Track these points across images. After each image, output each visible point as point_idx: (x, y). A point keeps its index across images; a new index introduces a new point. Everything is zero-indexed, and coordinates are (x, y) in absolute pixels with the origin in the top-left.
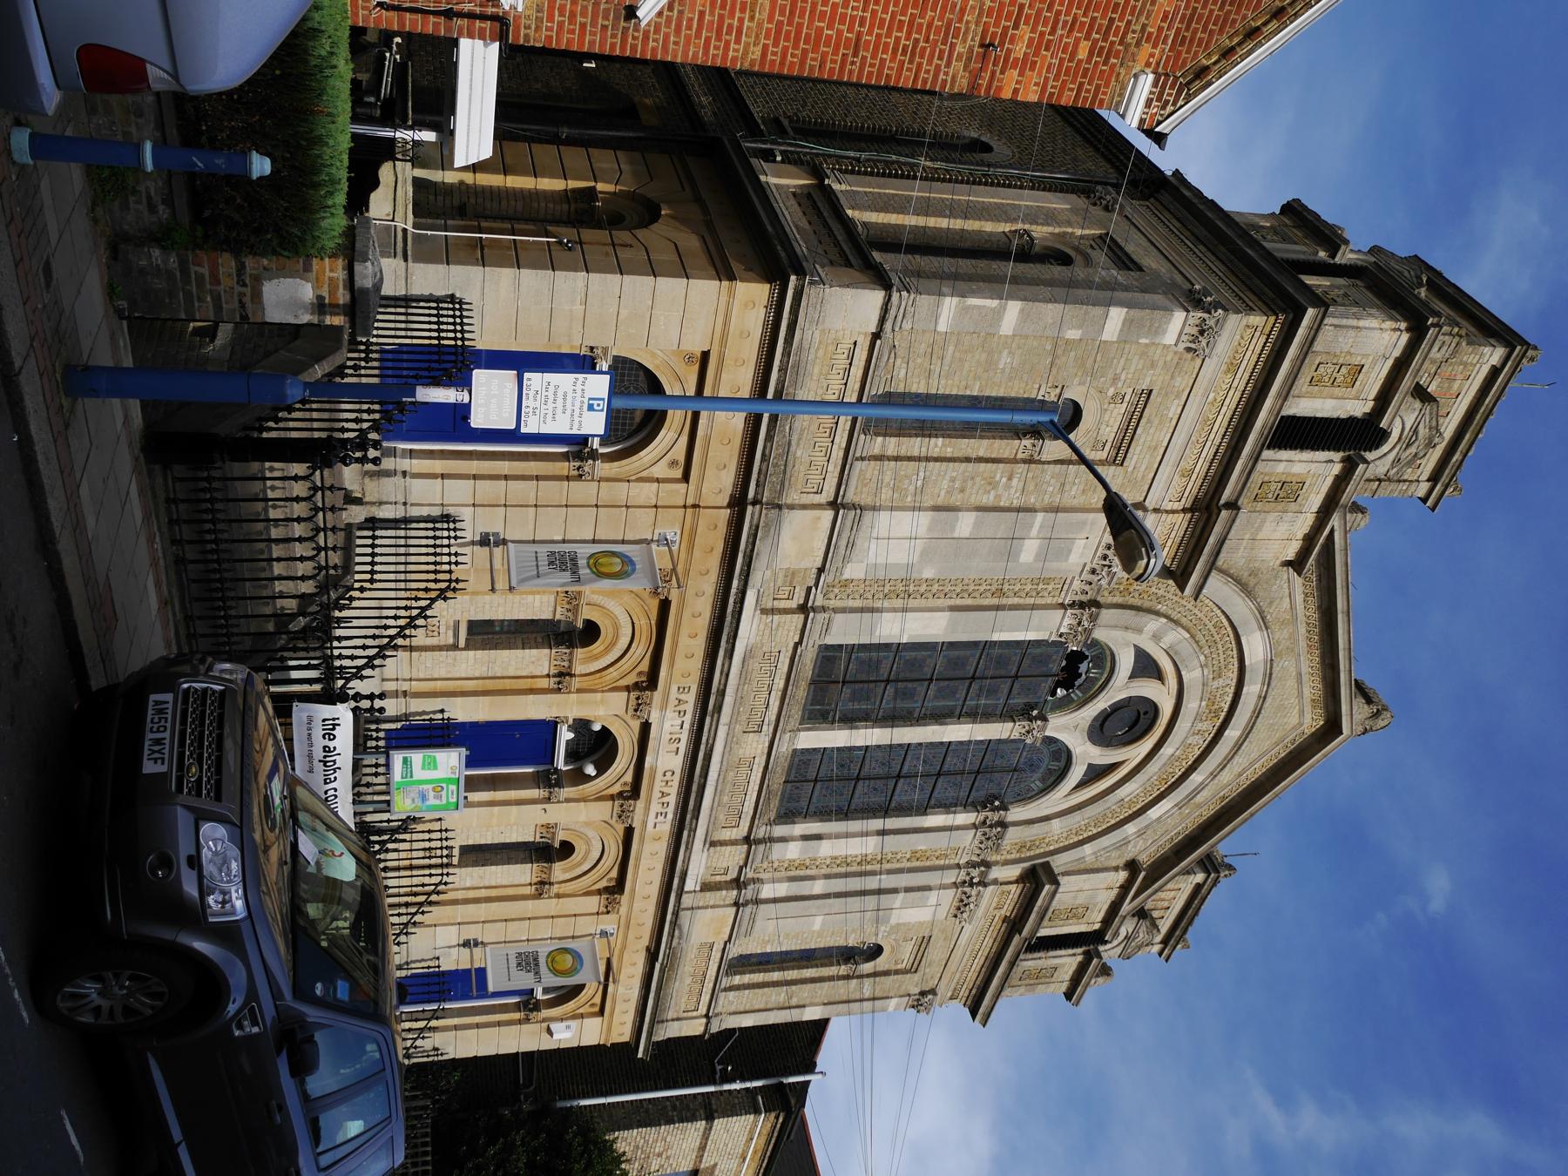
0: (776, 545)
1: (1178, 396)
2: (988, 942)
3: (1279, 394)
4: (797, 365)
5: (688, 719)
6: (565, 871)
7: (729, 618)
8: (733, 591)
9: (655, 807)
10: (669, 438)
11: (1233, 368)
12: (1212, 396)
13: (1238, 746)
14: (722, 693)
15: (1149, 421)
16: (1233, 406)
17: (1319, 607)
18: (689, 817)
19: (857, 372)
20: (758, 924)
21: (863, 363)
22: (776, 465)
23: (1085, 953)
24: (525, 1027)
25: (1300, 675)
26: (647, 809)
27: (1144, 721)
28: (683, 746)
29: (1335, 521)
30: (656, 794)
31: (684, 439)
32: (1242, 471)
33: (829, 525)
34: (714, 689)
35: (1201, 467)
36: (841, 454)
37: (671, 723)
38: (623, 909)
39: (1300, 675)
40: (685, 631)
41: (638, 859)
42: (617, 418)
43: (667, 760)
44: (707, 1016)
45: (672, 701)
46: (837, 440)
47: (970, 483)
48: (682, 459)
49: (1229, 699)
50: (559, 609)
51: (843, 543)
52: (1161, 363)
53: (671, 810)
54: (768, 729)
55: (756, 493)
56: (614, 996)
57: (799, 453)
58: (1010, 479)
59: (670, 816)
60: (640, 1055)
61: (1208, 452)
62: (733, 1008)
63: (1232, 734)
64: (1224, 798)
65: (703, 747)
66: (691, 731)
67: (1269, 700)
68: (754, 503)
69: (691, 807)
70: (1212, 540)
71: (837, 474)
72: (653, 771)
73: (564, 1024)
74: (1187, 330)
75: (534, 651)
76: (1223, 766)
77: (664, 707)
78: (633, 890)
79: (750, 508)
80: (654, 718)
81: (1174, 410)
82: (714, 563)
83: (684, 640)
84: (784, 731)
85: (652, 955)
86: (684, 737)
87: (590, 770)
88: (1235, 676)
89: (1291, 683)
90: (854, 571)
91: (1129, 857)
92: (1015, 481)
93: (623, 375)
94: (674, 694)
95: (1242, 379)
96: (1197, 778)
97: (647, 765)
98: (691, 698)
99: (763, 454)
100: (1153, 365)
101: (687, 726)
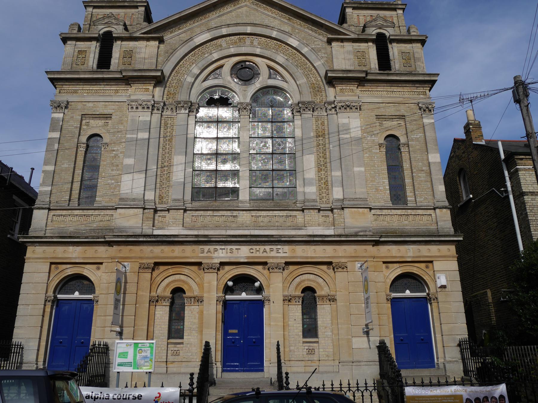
0: (131, 228)
1: (85, 105)
2: (379, 89)
3: (78, 74)
4: (59, 233)
5: (218, 247)
6: (322, 289)
7: (158, 239)
8: (145, 239)
9: (274, 254)
10: (87, 271)
11: (75, 92)
12: (85, 94)
13: (255, 25)
14: (197, 236)
15: (94, 111)
16: (89, 86)
17: (185, 23)
18: (272, 239)
19: (64, 212)
20: (358, 197)
21: (61, 211)
22: (99, 233)
23: (391, 43)
24: (439, 300)
25: (218, 17)
26: (273, 257)
27: (239, 66)
28: (234, 247)
29: (137, 35)
30: (265, 254)
31: (87, 266)
32: (109, 74)
33: (123, 210)
34: (196, 239)
35: (114, 88)
36: (97, 211)
37: (222, 254)
38: (343, 260)
39: (218, 17)
40: (171, 255)
41: (307, 258)
42: (91, 290)
43: (244, 253)
44: (434, 209)
45: (209, 254)
46: (91, 214)
47: (115, 164)
48: (96, 266)
49: (233, 37)
50: (164, 304)
51: (132, 203)
52: (72, 115)
53: (274, 247)
54: (235, 213)
55: (102, 238)
56: (413, 257)
57: (95, 226)
58: (114, 151)
59: (279, 247)
60: (461, 239)
61: (108, 88)
62: (431, 197)
63: (249, 30)
64: (289, 19)
65: (229, 239)
66: (225, 245)
67: (228, 22)
68: (105, 238)
69: (266, 239)
70: (135, 74)
71: (105, 211)
72: (248, 257)
73: (438, 280)
74: (55, 111)
75: (186, 312)
76: (267, 26)
77: (212, 258)
78: (329, 257)
79: (107, 239)
80: (218, 261)
81: (91, 105)
82: (137, 249)
83: (176, 254)
84: (238, 207)
85: (377, 243)
86: (229, 247)
87: (257, 284)
88: (220, 40)
89: (224, 18)
90: (150, 196)
91: (325, 45)
92: (115, 149)
93: (70, 289)
94: (205, 255)
95: (79, 87)
96: (274, 34)
97: (246, 261)
98: (206, 248)
99: (86, 238)
100: (72, 117)
101: (223, 247)
